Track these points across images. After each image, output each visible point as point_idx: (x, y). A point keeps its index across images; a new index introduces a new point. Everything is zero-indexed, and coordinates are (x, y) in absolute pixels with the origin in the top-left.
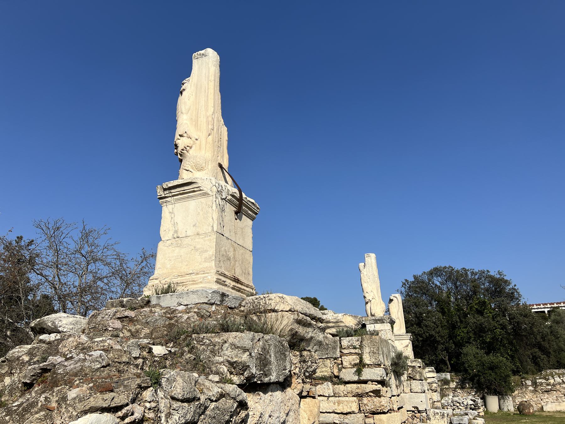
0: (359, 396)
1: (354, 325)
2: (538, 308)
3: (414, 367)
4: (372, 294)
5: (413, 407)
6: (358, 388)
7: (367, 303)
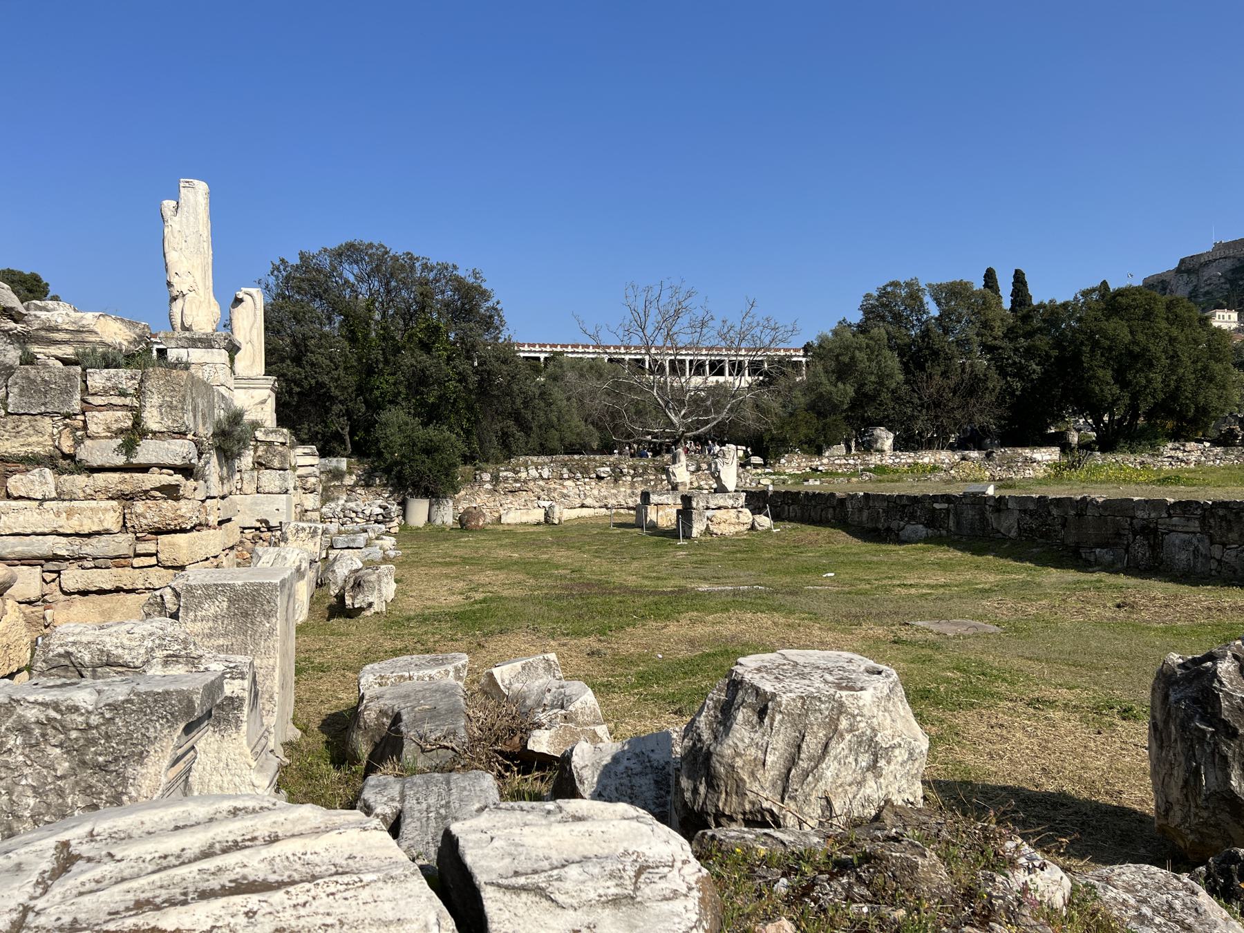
0: (126, 498)
1: (126, 343)
2: (530, 351)
3: (270, 444)
4: (190, 279)
5: (258, 520)
7: (174, 299)
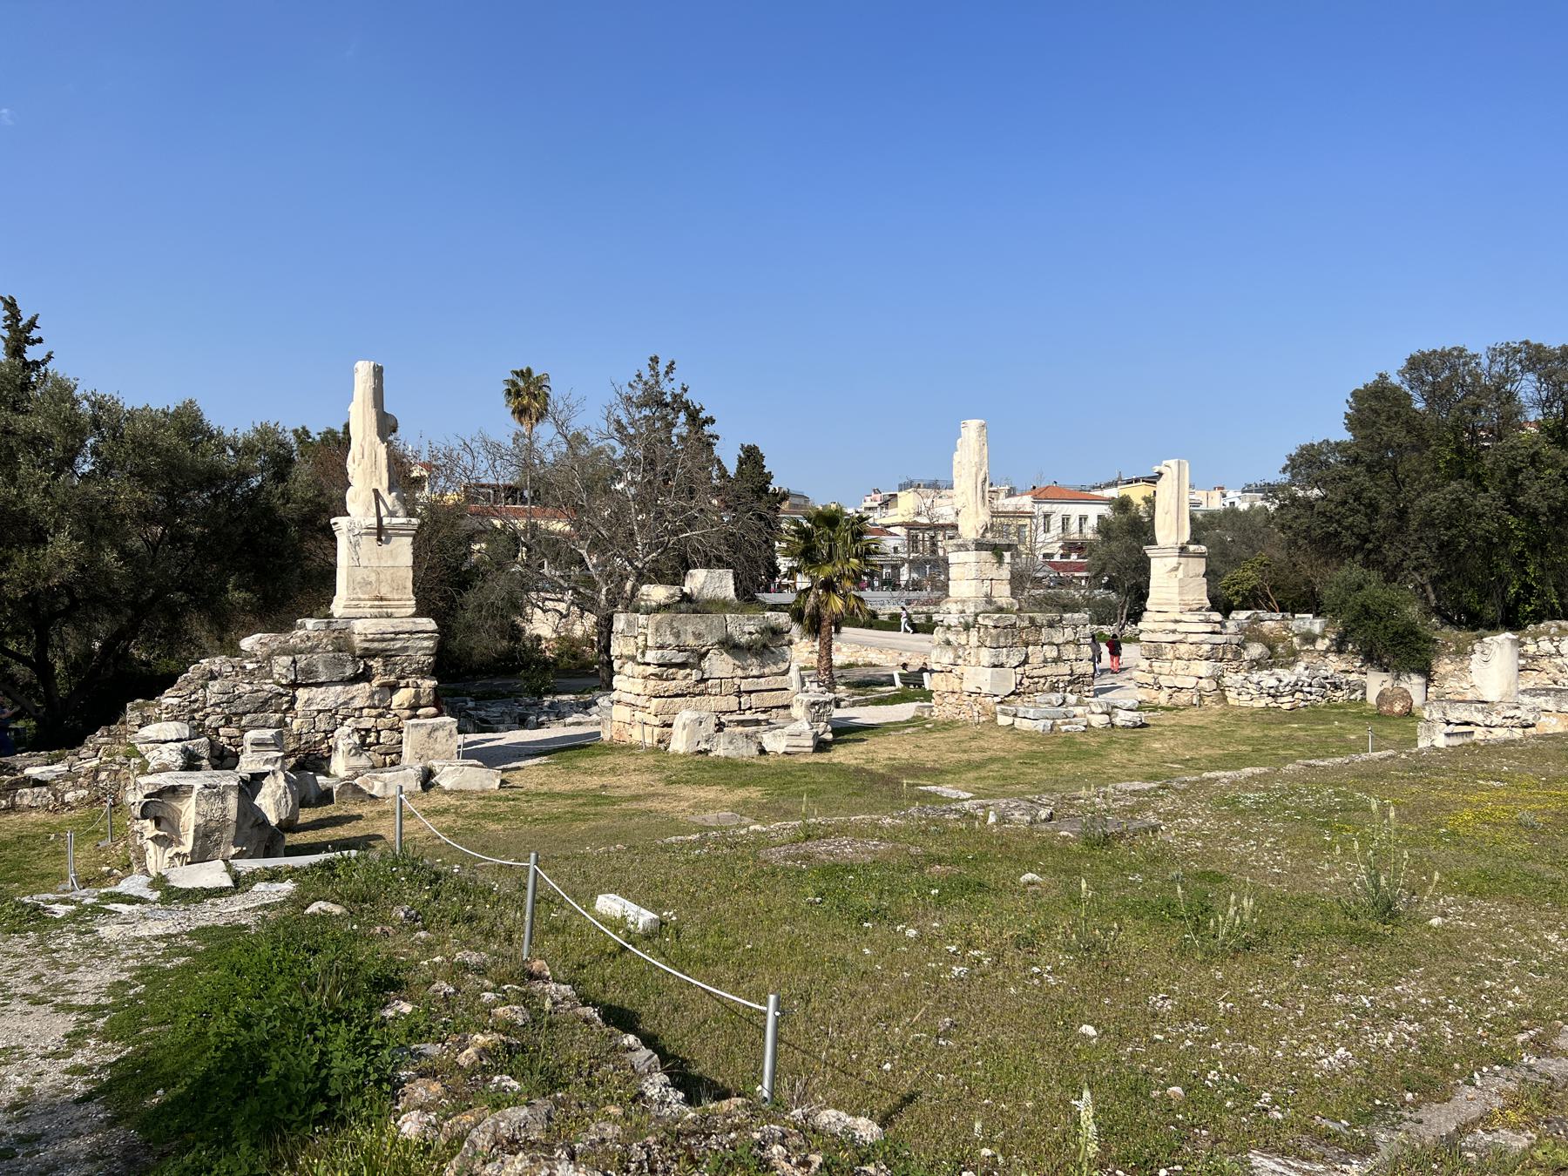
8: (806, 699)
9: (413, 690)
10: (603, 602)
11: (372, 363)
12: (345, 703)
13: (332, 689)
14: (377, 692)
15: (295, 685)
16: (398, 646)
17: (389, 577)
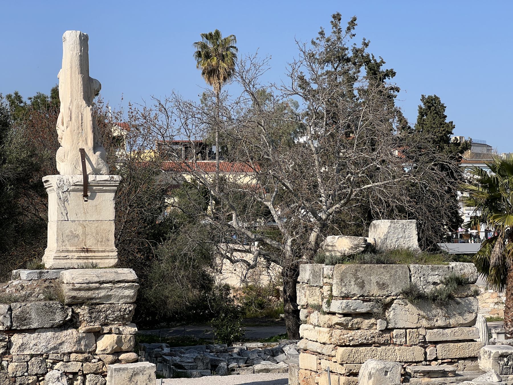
1: (348, 250)
6: (329, 320)
8: (494, 351)
9: (116, 336)
10: (288, 253)
11: (79, 32)
12: (55, 348)
13: (44, 335)
14: (83, 338)
15: (10, 331)
16: (102, 294)
17: (94, 231)
